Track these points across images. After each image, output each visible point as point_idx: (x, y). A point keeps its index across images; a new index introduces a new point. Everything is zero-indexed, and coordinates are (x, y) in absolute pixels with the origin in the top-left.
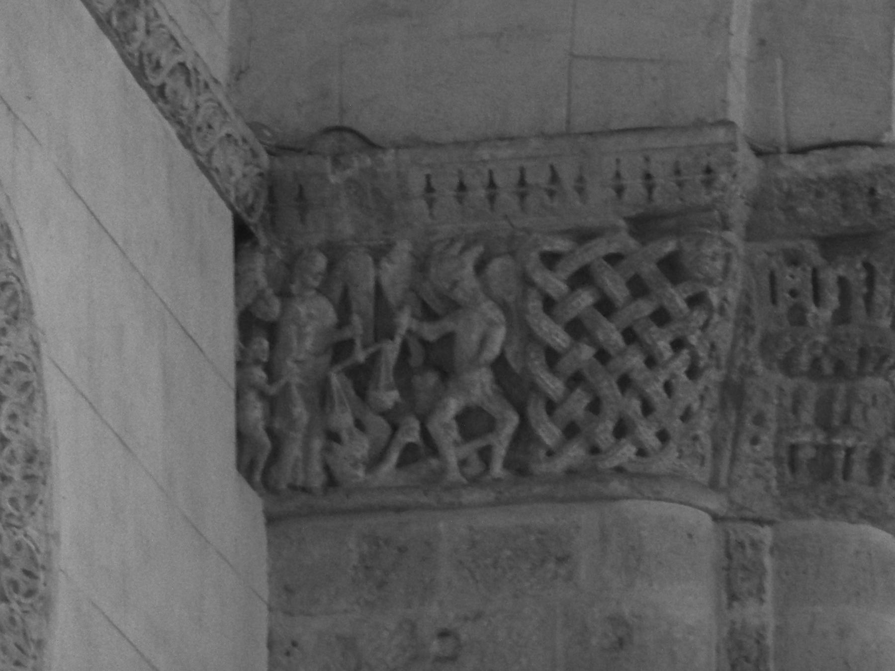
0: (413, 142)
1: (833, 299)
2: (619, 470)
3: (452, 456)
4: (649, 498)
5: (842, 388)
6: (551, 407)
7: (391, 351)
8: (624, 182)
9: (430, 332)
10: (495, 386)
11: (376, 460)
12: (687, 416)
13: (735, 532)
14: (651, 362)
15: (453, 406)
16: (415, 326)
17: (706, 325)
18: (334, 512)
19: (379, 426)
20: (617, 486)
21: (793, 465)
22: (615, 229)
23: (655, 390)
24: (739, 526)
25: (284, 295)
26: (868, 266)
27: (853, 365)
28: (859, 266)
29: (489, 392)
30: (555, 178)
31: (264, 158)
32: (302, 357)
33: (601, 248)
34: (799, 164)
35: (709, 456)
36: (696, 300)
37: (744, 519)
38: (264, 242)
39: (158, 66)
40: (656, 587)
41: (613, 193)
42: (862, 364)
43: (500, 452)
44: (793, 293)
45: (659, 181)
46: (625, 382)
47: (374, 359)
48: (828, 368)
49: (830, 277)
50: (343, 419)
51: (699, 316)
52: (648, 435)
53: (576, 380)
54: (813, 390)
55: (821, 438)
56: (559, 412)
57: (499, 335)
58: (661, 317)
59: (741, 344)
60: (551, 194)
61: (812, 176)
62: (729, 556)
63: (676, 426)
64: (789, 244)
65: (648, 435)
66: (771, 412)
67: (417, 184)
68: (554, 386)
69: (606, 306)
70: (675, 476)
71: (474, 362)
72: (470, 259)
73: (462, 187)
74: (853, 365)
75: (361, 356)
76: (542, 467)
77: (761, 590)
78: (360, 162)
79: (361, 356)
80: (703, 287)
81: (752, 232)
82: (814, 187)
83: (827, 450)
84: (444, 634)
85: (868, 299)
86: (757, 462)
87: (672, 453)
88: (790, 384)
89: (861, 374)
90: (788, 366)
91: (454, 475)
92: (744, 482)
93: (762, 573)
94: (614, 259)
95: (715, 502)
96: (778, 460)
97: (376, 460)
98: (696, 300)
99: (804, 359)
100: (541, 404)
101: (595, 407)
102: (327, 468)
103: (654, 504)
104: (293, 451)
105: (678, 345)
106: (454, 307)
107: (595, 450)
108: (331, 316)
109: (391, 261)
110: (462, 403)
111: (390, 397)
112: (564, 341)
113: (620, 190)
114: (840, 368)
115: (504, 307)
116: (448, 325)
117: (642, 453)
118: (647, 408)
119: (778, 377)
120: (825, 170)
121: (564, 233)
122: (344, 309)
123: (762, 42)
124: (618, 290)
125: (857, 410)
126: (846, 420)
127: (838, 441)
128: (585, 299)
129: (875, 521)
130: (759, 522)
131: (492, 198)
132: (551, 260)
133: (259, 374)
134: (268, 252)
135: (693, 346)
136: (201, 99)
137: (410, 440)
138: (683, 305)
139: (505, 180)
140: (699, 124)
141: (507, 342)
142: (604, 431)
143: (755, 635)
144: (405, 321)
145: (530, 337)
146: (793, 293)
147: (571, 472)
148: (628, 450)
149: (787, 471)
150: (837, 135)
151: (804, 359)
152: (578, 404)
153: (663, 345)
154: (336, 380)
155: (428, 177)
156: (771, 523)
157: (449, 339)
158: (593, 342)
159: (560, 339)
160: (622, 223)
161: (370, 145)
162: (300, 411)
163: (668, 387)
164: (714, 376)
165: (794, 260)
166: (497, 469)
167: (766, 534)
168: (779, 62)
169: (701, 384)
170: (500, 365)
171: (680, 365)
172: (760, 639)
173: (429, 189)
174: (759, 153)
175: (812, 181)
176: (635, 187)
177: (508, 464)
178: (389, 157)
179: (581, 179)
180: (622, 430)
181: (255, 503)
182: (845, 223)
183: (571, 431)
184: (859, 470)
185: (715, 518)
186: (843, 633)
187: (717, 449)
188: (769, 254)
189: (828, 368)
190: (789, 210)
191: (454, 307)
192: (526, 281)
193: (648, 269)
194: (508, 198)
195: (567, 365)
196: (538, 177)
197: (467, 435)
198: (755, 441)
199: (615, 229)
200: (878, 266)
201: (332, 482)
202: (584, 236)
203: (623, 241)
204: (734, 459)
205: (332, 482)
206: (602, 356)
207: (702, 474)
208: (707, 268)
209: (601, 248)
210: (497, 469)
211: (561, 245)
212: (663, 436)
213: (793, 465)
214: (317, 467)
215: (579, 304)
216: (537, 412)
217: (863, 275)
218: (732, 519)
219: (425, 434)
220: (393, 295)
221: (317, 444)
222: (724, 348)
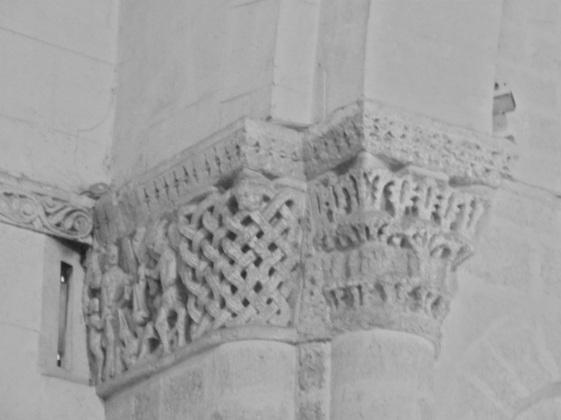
5: (354, 253)
24: (307, 346)
26: (352, 178)
32: (111, 303)
37: (310, 341)
38: (96, 246)
42: (358, 236)
59: (305, 240)
61: (320, 135)
67: (141, 196)
74: (354, 238)
77: (321, 380)
80: (246, 214)
85: (357, 196)
86: (313, 306)
95: (292, 335)
103: (237, 343)
104: (110, 356)
105: (246, 248)
109: (136, 241)
110: (167, 310)
112: (195, 262)
113: (209, 170)
117: (234, 315)
129: (381, 326)
143: (315, 409)
146: (327, 204)
156: (329, 340)
167: (327, 348)
172: (318, 410)
175: (321, 138)
179: (194, 170)
188: (317, 185)
189: (344, 243)
190: (317, 157)
199: (210, 193)
200: (355, 176)
208: (244, 202)
212: (246, 303)
214: (119, 363)
217: (351, 184)
218: (303, 342)
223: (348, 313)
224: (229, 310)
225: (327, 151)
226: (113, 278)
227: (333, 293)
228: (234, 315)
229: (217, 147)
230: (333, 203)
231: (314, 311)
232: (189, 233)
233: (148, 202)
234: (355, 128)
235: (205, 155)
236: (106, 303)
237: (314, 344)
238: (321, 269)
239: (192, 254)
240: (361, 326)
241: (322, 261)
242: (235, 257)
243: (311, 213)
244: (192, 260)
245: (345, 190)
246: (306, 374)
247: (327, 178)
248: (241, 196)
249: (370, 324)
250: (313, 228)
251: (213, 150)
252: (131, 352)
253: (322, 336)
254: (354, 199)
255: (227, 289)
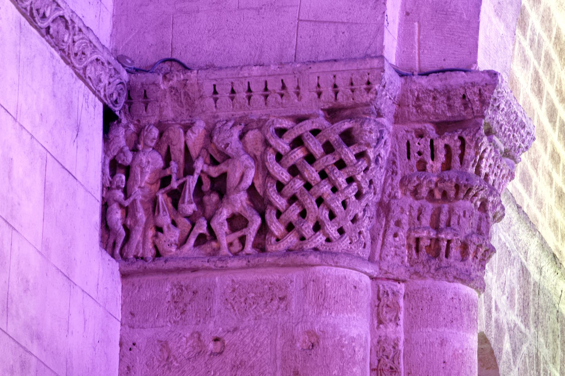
0: (210, 67)
1: (441, 156)
2: (316, 249)
3: (224, 241)
4: (331, 265)
5: (446, 207)
6: (279, 214)
7: (192, 181)
8: (321, 89)
9: (214, 172)
10: (248, 202)
11: (183, 242)
12: (355, 220)
13: (383, 286)
14: (335, 190)
15: (225, 213)
16: (205, 168)
17: (367, 169)
18: (158, 271)
19: (184, 223)
20: (313, 258)
21: (418, 250)
22: (318, 116)
23: (337, 206)
24: (385, 283)
25: (135, 150)
26: (461, 138)
27: (452, 194)
28: (456, 138)
29: (245, 204)
30: (284, 87)
31: (125, 75)
32: (143, 185)
33: (308, 126)
34: (424, 81)
35: (369, 243)
36: (361, 155)
37: (388, 279)
38: (124, 121)
39: (44, 16)
40: (333, 314)
41: (316, 95)
42: (457, 194)
43: (250, 239)
44: (420, 153)
45: (341, 88)
46: (320, 201)
47: (182, 186)
48: (438, 195)
49: (440, 144)
50: (165, 219)
51: (363, 164)
52: (332, 229)
53: (293, 199)
54: (430, 207)
55: (433, 234)
56: (283, 217)
57: (251, 174)
58: (341, 165)
59: (389, 181)
60: (282, 95)
61: (430, 88)
62: (379, 299)
63: (348, 225)
64: (418, 126)
65: (332, 229)
66: (405, 219)
67: (208, 89)
68: (280, 202)
69: (310, 159)
70: (348, 253)
71: (237, 189)
72: (236, 133)
73: (233, 91)
74: (452, 194)
75: (175, 185)
76: (272, 247)
77: (397, 318)
78: (177, 78)
79: (175, 185)
80: (364, 148)
81: (398, 119)
82: (432, 94)
83: (438, 240)
84: (216, 340)
85: (462, 156)
86: (395, 247)
87: (346, 241)
88: (416, 204)
89: (456, 197)
90: (415, 193)
91: (225, 251)
92: (389, 258)
93: (398, 309)
94: (315, 132)
95: (371, 269)
96: (409, 247)
97: (183, 242)
98: (361, 155)
99: (424, 191)
100: (274, 212)
101: (303, 214)
102: (155, 247)
103: (334, 268)
104: (137, 237)
105: (350, 180)
106: (227, 157)
107: (302, 238)
108: (160, 163)
109: (193, 132)
110: (230, 212)
111: (190, 208)
112: (286, 177)
113: (319, 94)
114: (444, 194)
115: (254, 158)
116: (223, 167)
117: (328, 240)
118: (332, 216)
119: (410, 199)
120: (438, 84)
121: (287, 117)
122: (167, 159)
123: (408, 14)
124: (317, 149)
125: (454, 220)
126: (448, 225)
127: (443, 236)
128: (299, 154)
129: (463, 282)
130: (397, 280)
131: (249, 98)
132: (281, 132)
133: (119, 194)
134: (127, 127)
135: (359, 181)
136: (76, 38)
137: (201, 232)
138: (353, 158)
139: (257, 88)
140: (366, 57)
141: (256, 177)
142: (307, 228)
143: (392, 344)
144: (200, 165)
145: (268, 175)
146: (420, 153)
147: (289, 250)
148: (320, 239)
149: (414, 252)
150: (446, 66)
151: (424, 191)
152: (293, 212)
153: (341, 180)
154: (162, 198)
155: (215, 86)
156: (404, 281)
157: (224, 176)
158: (303, 178)
159: (284, 176)
160: (321, 112)
161: (186, 68)
162: (141, 215)
163: (344, 204)
164: (371, 198)
165: (421, 135)
166: (249, 248)
167: (401, 288)
168: (416, 24)
169: (364, 203)
170: (251, 190)
171: (352, 190)
172: (395, 346)
173: (215, 92)
174: (401, 75)
175: (430, 91)
176: (328, 92)
177: (255, 246)
178: (193, 75)
179: (298, 88)
180: (317, 227)
181: (115, 266)
182: (449, 114)
183: (290, 227)
184: (455, 252)
185: (372, 278)
186: (443, 342)
187: (373, 239)
188: (407, 131)
189: (438, 195)
190: (418, 107)
191: (227, 157)
192: (267, 144)
193: (334, 138)
194: (257, 97)
195: (288, 191)
196: (273, 86)
197: (233, 229)
198: (395, 235)
199: (318, 116)
200: (467, 138)
201: (158, 254)
202: (299, 119)
203: (321, 122)
204: (383, 244)
205: (158, 254)
206: (308, 186)
207: (366, 253)
208: (367, 137)
209: (308, 126)
210: (249, 248)
211: (286, 124)
212: (341, 231)
213: (418, 250)
214: (150, 246)
215: (295, 156)
216: (271, 216)
217: (459, 144)
218: (382, 279)
219: (209, 228)
220: (194, 152)
221: (151, 233)
222: (378, 183)
223: (433, 261)
224: (324, 234)
225: (434, 105)
226: (150, 160)
227: (418, 240)
228: (328, 240)
229: (339, 75)
230: (428, 153)
231: (396, 251)
232: (283, 147)
233: (216, 100)
234: (480, 94)
235: (318, 77)
236: (139, 183)
237: (390, 282)
238: (408, 213)
239: (283, 169)
240: (446, 277)
241: (411, 206)
242: (341, 186)
243: (398, 158)
244: (282, 174)
245: (447, 147)
246: (384, 309)
247: (424, 128)
248: (366, 131)
249: (455, 277)
250: (400, 172)
251: (332, 77)
252: (173, 239)
253: (402, 277)
254: (457, 158)
255: (325, 214)
